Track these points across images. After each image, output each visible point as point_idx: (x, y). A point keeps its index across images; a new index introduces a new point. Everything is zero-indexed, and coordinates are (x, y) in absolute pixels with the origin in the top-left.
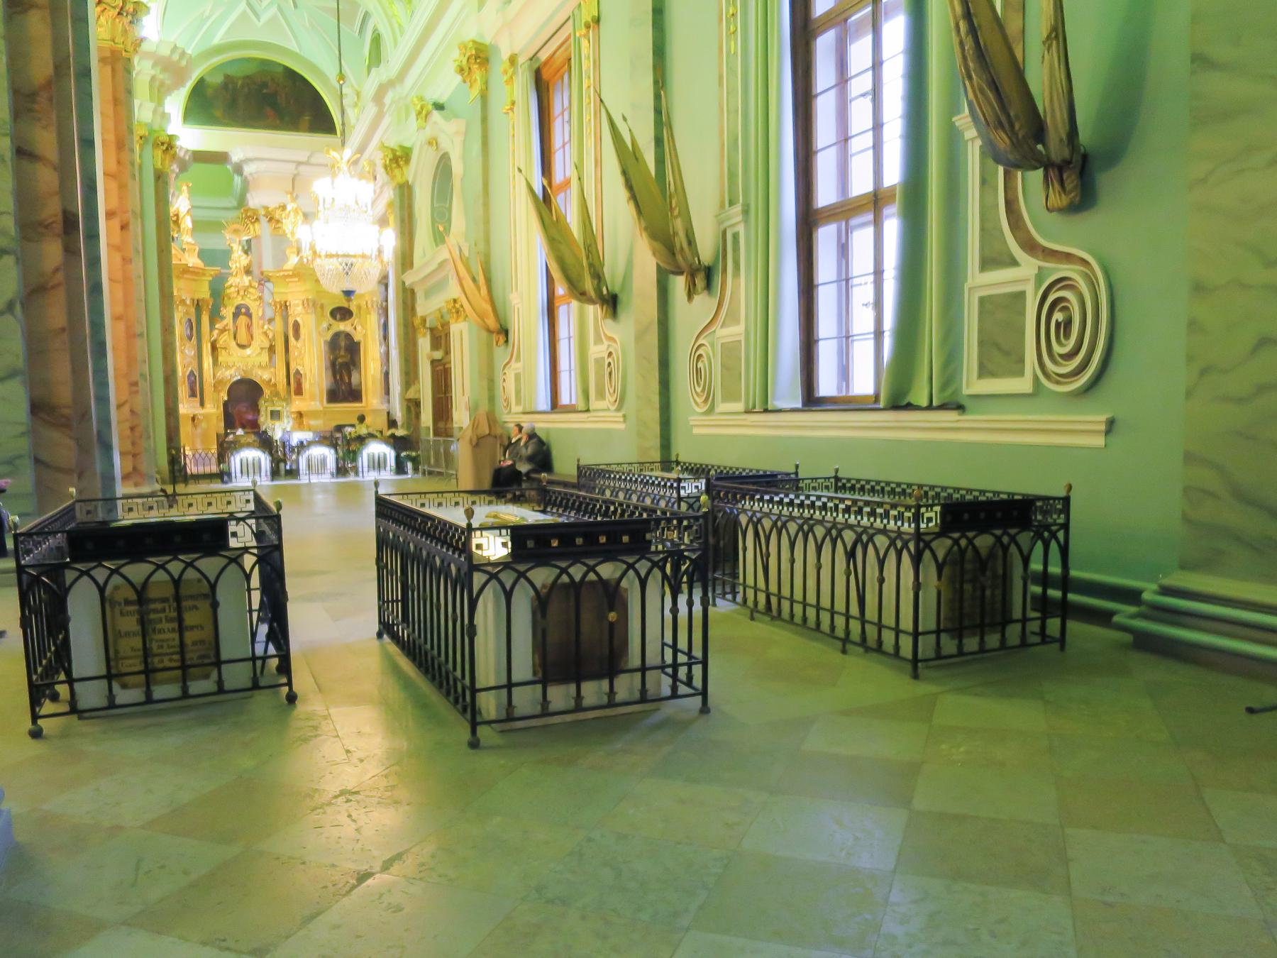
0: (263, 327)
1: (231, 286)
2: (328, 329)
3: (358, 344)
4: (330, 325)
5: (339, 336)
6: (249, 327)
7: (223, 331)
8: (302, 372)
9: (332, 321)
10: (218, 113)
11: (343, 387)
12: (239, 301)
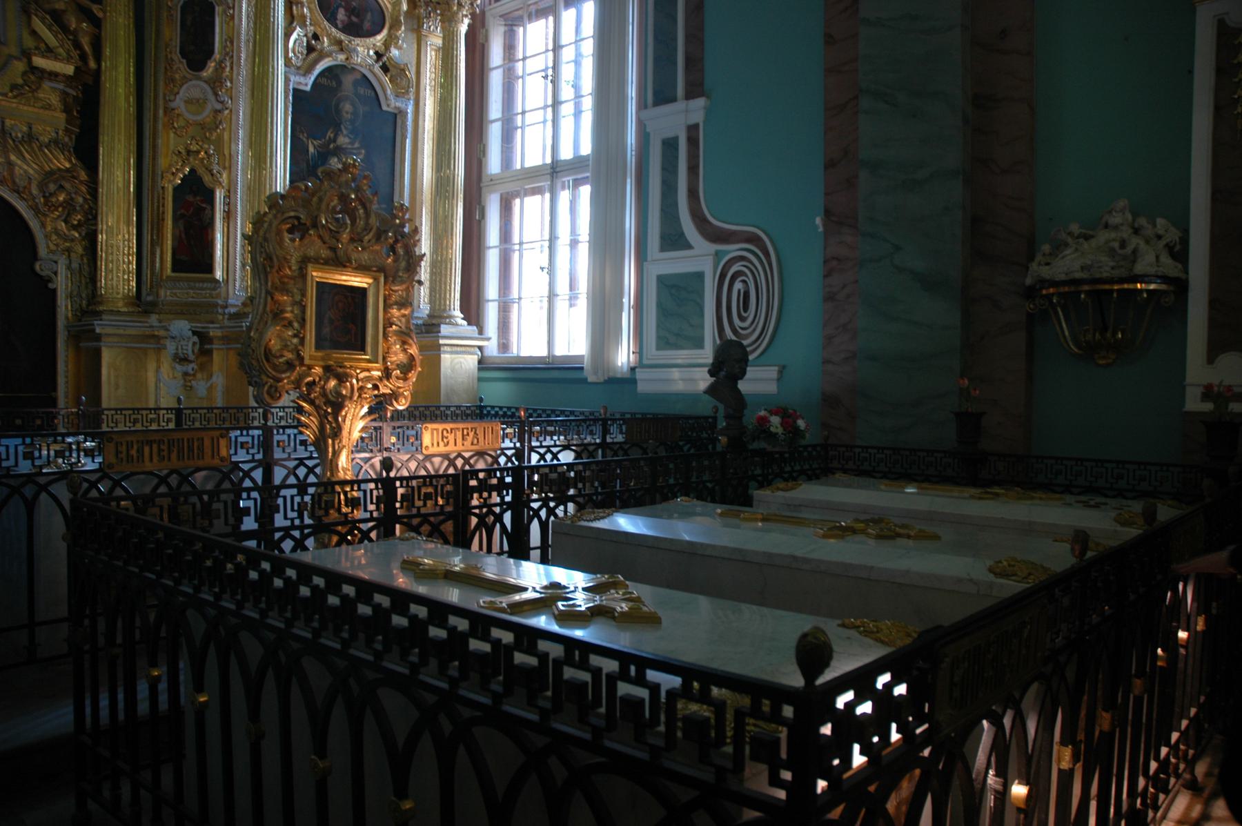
5: (339, 83)
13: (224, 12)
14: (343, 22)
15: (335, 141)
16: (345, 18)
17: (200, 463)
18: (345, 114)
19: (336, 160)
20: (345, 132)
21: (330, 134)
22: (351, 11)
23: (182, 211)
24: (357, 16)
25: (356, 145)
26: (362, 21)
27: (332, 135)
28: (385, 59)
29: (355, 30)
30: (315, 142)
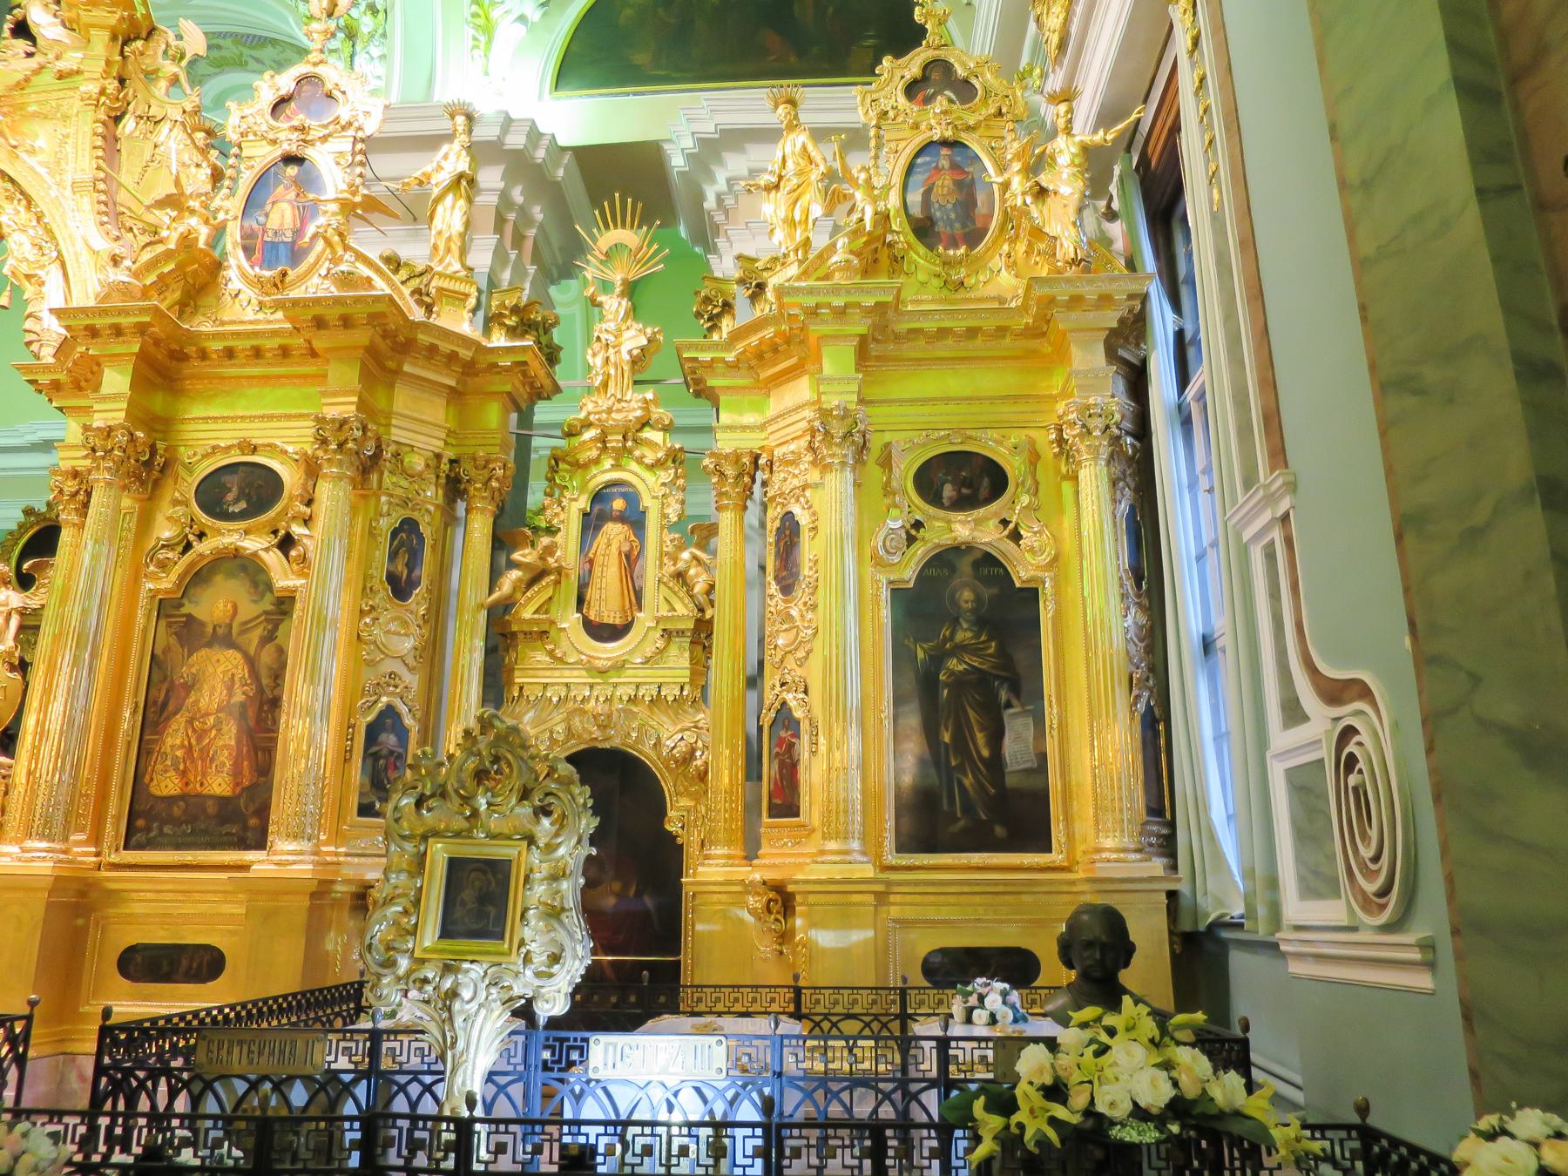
0: (675, 560)
1: (587, 425)
2: (911, 540)
3: (1031, 596)
4: (918, 525)
5: (953, 569)
6: (631, 561)
7: (537, 576)
8: (798, 714)
9: (922, 510)
10: (641, 58)
11: (968, 781)
12: (604, 473)
14: (950, 498)
16: (954, 493)
17: (292, 1071)
18: (965, 606)
19: (955, 661)
20: (965, 626)
21: (945, 632)
22: (960, 483)
23: (777, 749)
24: (970, 486)
25: (983, 638)
26: (976, 491)
28: (1011, 526)
29: (965, 502)
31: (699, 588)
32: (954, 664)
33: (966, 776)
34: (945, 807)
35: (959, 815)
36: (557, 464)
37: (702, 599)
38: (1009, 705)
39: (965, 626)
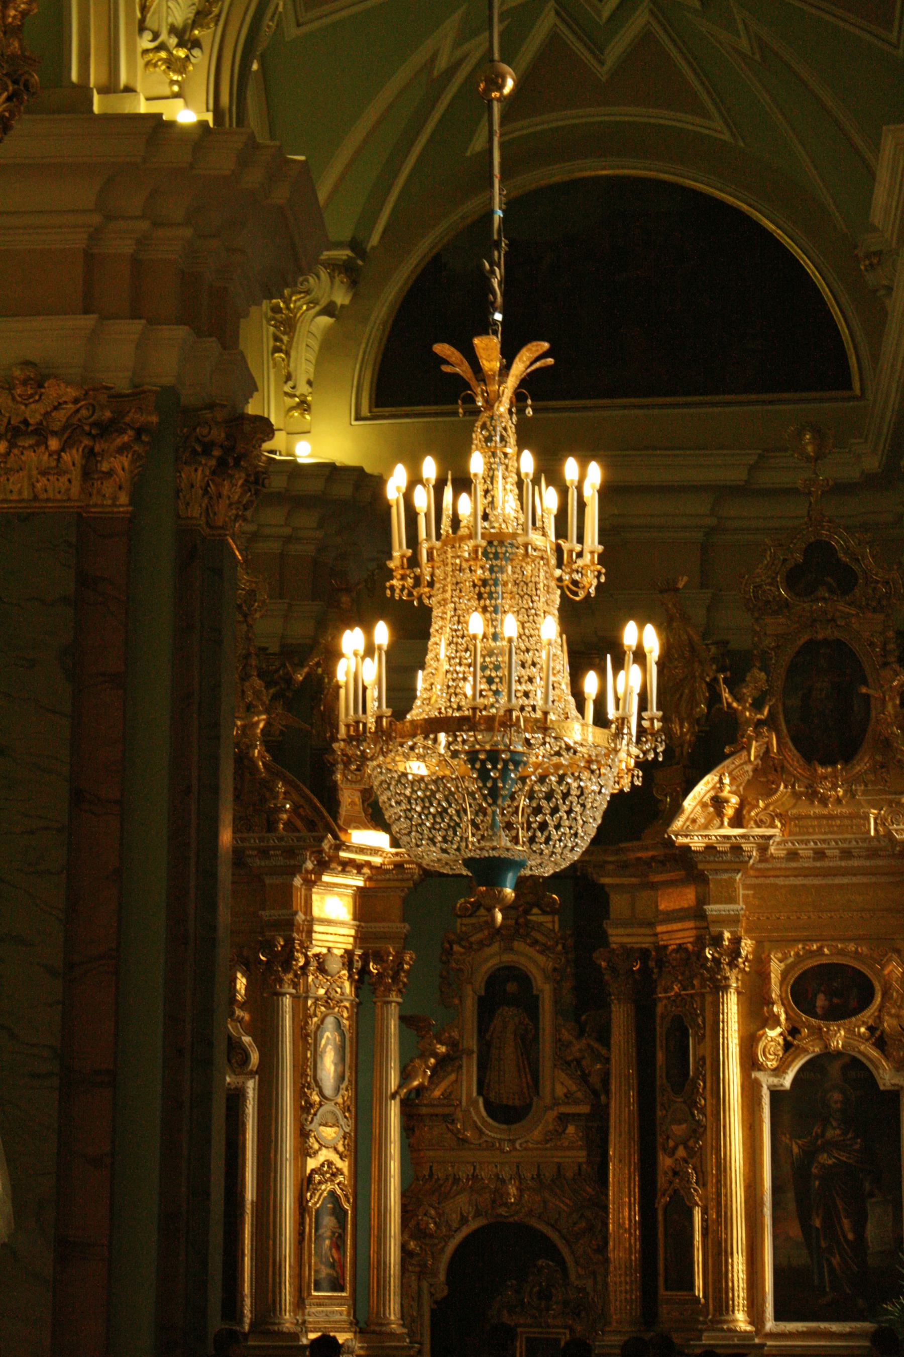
11: (836, 1261)
13: (696, 1033)
14: (823, 1008)
15: (823, 1135)
19: (825, 1155)
20: (834, 1124)
21: (817, 1129)
25: (850, 1136)
27: (819, 1131)
28: (878, 1033)
29: (836, 1014)
30: (800, 1142)
31: (594, 1080)
32: (824, 1158)
33: (835, 1257)
34: (816, 1282)
35: (828, 1290)
36: (452, 948)
37: (598, 1086)
38: (872, 1195)
39: (834, 1124)
